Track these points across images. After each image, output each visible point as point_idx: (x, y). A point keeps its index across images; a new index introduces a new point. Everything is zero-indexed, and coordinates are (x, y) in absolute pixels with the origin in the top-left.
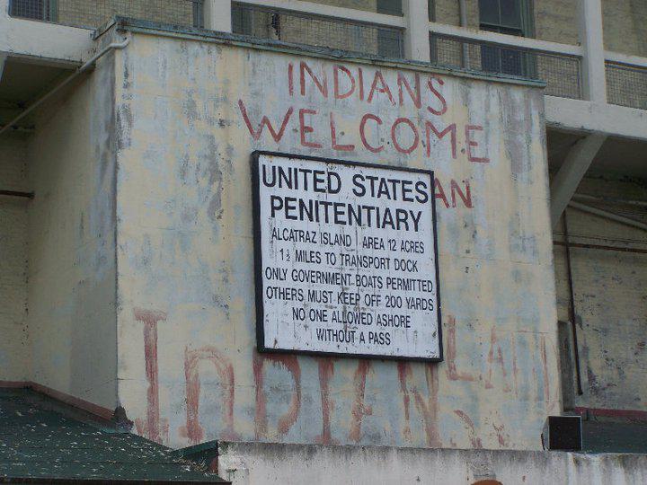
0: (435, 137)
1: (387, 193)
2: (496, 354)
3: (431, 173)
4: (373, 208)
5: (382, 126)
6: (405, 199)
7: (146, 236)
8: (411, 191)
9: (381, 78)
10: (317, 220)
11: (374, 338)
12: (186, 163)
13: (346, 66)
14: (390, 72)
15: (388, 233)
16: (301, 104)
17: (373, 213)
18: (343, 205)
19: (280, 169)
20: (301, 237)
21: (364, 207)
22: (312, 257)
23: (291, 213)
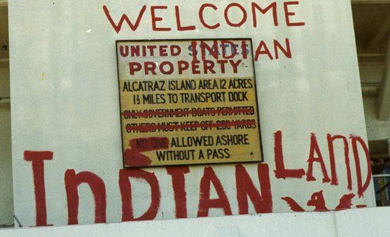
22: (157, 99)
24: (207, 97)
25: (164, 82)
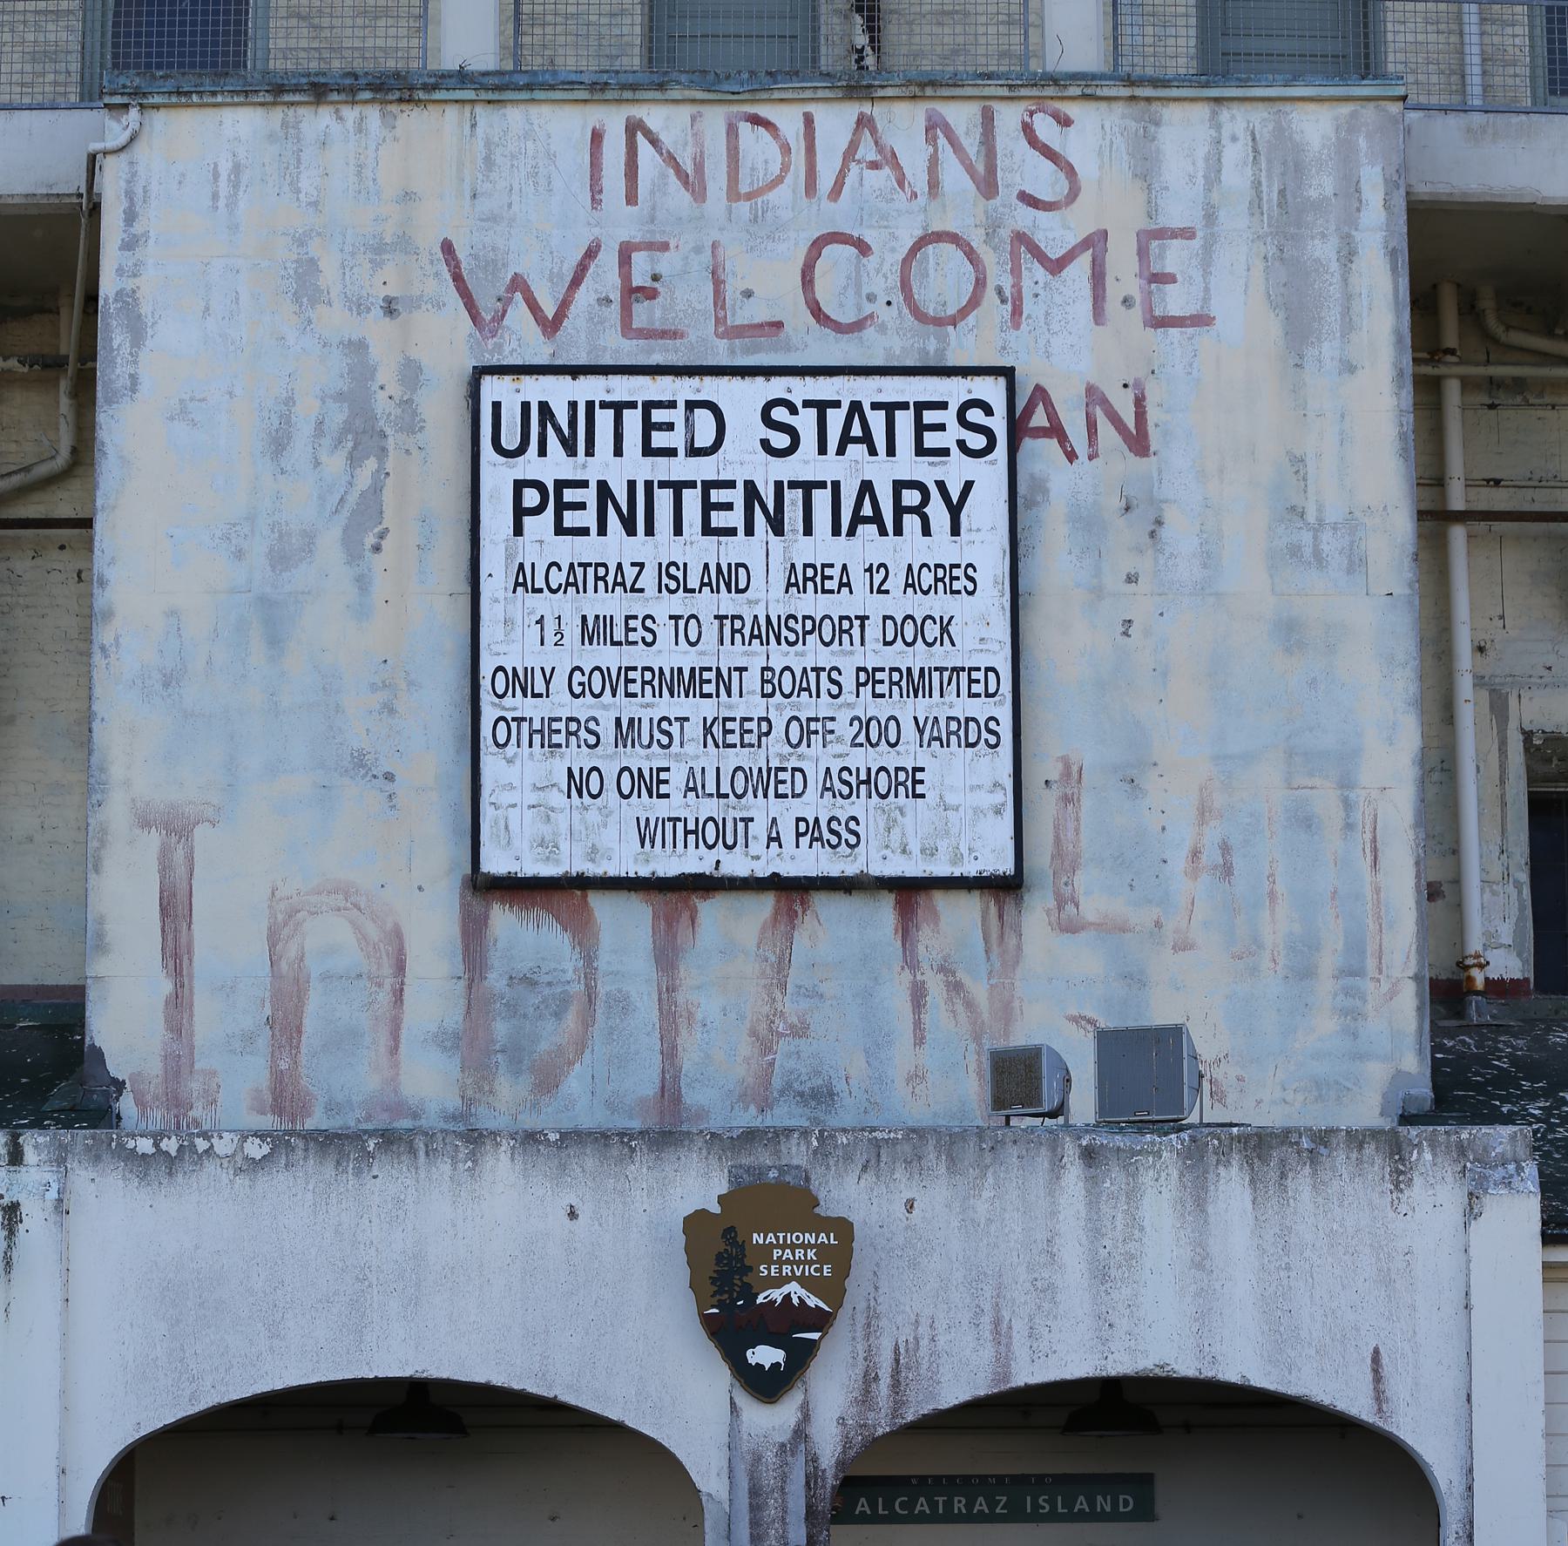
0: (1040, 273)
1: (867, 439)
2: (1211, 856)
3: (1008, 373)
4: (822, 485)
5: (871, 262)
6: (921, 451)
7: (173, 613)
8: (941, 427)
9: (873, 131)
10: (650, 531)
11: (808, 830)
12: (286, 419)
13: (764, 111)
14: (902, 110)
15: (868, 546)
16: (622, 224)
17: (822, 499)
18: (731, 484)
19: (545, 408)
20: (597, 578)
21: (793, 485)
22: (628, 630)
23: (571, 519)
24: (806, 633)
25: (642, 565)
